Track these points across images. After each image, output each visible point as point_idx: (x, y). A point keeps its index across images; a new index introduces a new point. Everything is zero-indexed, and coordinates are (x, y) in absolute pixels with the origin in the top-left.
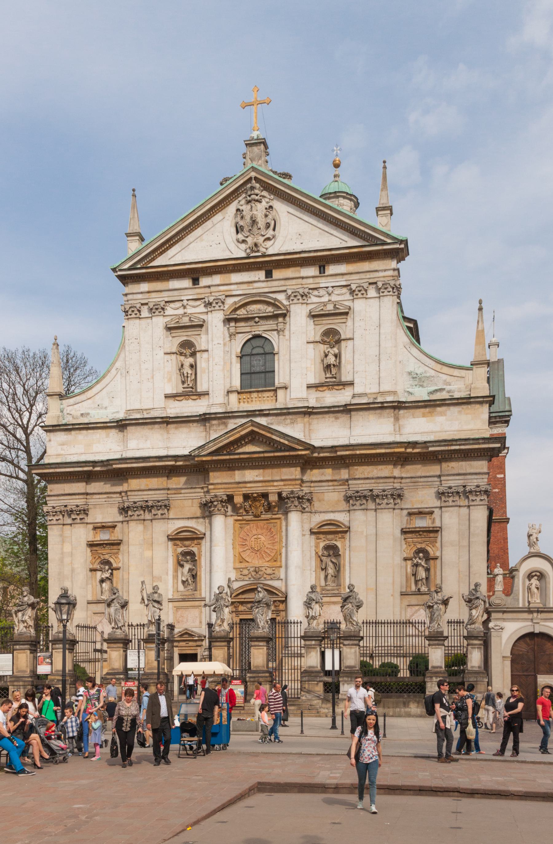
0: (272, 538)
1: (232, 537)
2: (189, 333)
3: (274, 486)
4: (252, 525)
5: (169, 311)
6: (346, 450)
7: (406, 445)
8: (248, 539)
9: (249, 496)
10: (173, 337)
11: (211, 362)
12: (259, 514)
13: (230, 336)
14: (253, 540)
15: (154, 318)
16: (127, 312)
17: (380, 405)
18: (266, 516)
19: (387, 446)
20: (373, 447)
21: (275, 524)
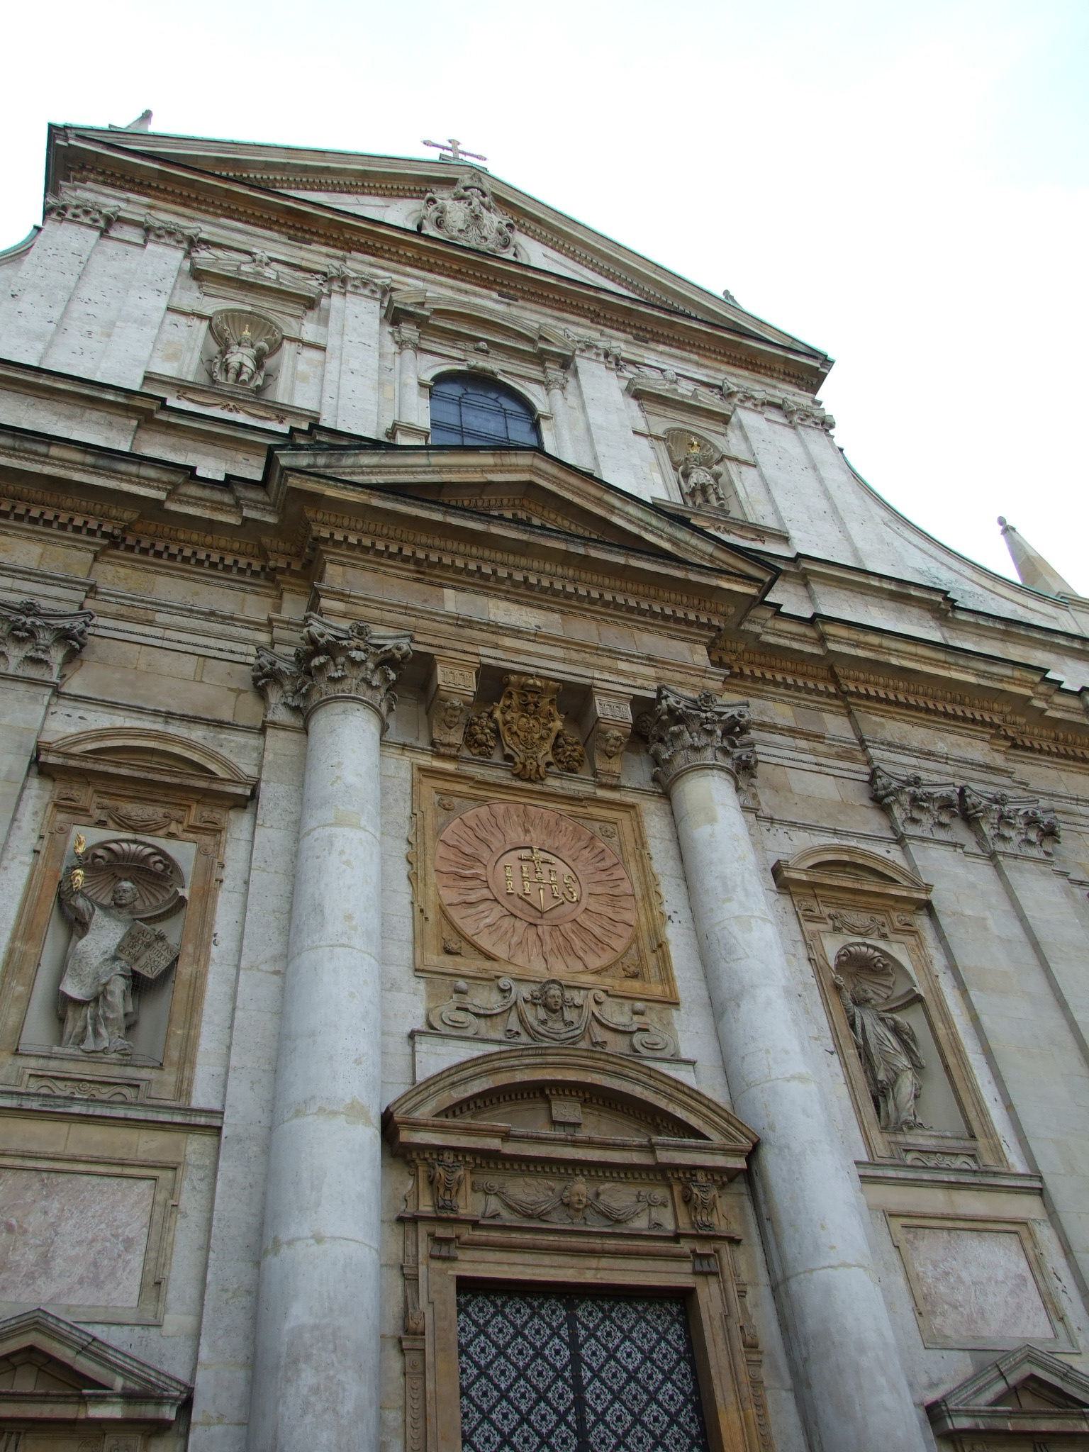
0: (604, 876)
1: (406, 831)
2: (266, 305)
3: (618, 672)
4: (500, 809)
5: (204, 256)
6: (858, 645)
7: (1037, 679)
8: (485, 854)
9: (508, 684)
10: (206, 294)
11: (333, 366)
12: (543, 766)
13: (401, 344)
14: (518, 863)
15: (150, 246)
16: (65, 208)
17: (893, 587)
18: (566, 784)
19: (982, 666)
20: (941, 656)
21: (609, 827)
